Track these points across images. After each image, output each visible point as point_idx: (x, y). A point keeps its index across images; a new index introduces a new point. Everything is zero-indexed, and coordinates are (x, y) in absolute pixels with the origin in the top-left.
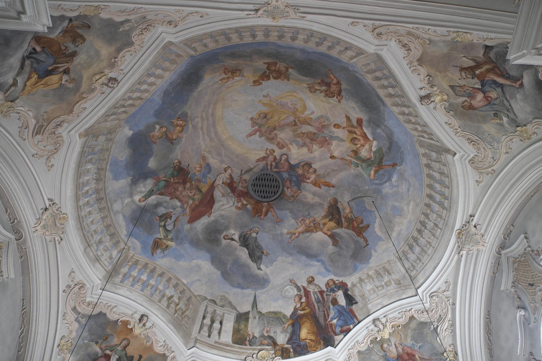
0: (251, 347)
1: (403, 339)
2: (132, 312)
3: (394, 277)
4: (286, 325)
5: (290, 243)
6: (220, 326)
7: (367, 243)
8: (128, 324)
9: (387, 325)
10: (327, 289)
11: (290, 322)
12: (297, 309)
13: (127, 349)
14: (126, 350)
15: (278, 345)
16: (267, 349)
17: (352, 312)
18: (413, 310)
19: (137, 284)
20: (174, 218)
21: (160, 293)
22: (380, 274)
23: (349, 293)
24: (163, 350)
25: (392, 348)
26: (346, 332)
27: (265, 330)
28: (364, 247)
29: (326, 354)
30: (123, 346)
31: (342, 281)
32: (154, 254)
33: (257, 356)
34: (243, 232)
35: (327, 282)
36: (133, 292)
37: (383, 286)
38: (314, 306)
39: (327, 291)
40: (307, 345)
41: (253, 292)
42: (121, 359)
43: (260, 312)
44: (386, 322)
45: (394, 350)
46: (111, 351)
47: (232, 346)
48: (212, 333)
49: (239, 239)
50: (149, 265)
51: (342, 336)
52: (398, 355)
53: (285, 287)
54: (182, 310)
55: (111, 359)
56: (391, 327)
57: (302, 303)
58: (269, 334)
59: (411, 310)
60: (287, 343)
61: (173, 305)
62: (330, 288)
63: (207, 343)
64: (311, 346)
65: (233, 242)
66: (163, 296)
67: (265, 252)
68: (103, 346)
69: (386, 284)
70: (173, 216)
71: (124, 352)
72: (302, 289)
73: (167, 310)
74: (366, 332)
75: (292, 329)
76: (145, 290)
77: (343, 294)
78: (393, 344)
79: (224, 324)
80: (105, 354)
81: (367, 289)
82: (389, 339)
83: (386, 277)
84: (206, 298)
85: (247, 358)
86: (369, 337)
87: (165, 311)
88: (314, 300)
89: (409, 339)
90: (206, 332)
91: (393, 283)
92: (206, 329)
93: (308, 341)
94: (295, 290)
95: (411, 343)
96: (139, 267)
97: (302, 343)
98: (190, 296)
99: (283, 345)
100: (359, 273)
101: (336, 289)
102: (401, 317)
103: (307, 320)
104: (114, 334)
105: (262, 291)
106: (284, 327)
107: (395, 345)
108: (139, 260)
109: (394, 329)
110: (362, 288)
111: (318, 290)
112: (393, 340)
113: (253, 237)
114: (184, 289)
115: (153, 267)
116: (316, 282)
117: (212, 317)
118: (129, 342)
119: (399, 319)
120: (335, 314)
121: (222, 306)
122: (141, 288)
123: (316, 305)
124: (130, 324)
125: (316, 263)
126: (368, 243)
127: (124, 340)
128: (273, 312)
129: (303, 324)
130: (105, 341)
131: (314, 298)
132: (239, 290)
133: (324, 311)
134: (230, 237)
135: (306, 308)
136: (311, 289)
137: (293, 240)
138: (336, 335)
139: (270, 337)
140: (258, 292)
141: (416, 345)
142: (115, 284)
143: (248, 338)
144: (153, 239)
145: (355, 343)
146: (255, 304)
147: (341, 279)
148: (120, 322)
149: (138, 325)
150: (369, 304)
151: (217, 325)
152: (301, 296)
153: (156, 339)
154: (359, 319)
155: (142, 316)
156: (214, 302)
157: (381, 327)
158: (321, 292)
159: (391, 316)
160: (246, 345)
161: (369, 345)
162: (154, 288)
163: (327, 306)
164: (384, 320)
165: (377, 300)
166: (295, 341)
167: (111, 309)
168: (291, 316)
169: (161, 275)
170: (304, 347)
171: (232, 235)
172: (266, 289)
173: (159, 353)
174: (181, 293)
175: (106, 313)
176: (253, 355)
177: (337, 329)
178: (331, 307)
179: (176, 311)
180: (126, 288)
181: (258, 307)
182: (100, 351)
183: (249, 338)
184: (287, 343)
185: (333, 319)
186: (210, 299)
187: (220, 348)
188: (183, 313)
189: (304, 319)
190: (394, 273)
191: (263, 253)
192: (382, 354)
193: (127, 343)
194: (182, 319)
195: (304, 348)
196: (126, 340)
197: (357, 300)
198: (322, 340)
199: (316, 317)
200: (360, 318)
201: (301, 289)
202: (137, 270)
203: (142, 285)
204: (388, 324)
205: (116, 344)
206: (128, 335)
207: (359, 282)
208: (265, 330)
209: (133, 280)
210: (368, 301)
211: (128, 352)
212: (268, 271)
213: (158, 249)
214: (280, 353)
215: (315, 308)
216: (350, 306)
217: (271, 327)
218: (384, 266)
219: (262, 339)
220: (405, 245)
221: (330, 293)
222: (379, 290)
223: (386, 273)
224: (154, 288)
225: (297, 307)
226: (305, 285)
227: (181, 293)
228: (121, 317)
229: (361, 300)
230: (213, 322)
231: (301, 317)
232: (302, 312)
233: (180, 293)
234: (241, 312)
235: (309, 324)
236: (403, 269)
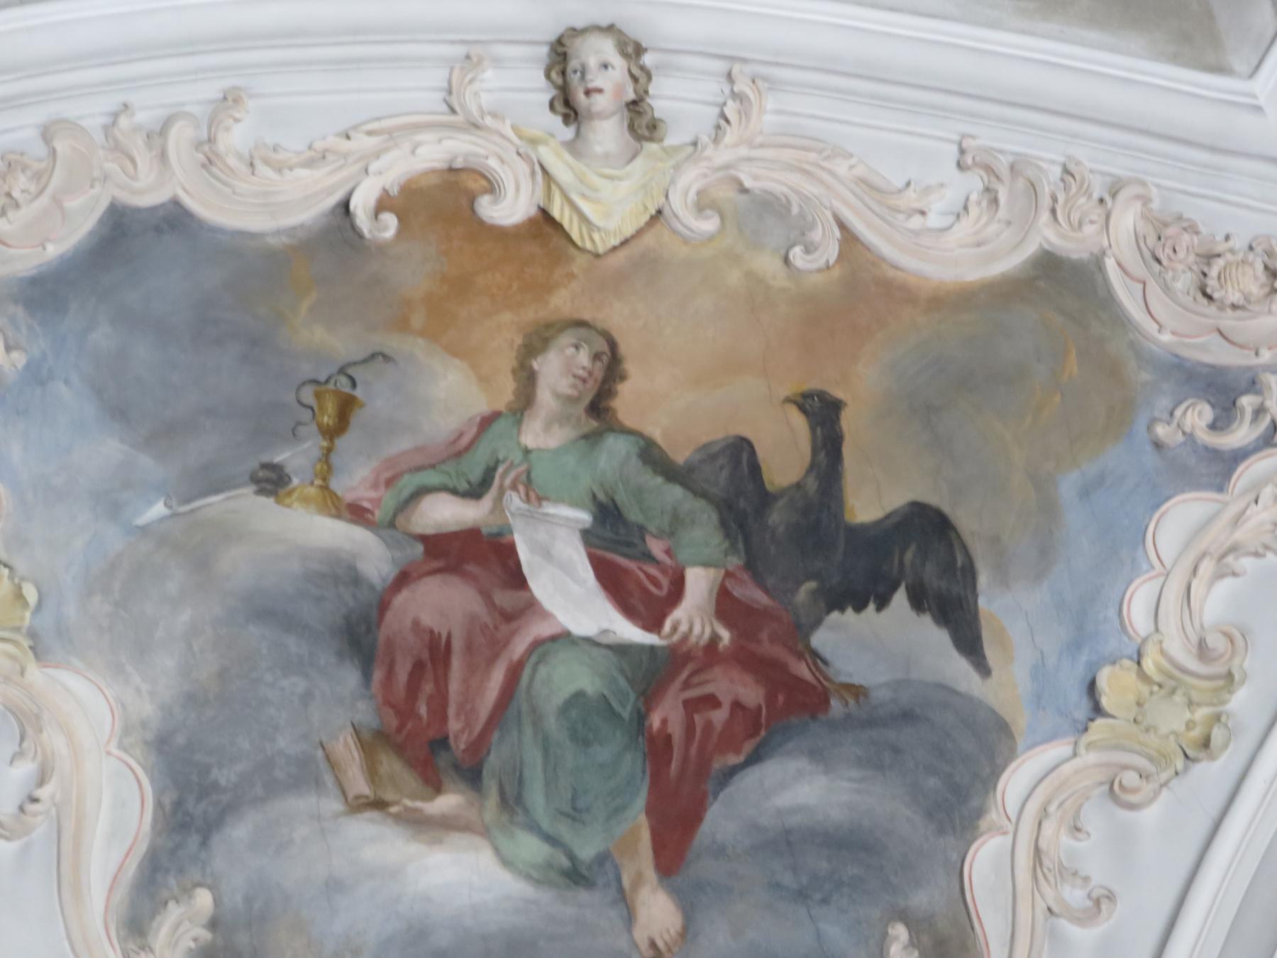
2: (438, 77)
13: (625, 403)
30: (571, 400)
42: (634, 515)
46: (475, 492)
71: (617, 448)
80: (424, 539)
104: (392, 343)
118: (602, 346)
124: (492, 187)
130: (342, 442)
149: (573, 146)
153: (867, 185)
167: (198, 146)
175: (176, 202)
193: (584, 358)
196: (566, 339)
205: (480, 405)
206: (547, 288)
211: (656, 433)
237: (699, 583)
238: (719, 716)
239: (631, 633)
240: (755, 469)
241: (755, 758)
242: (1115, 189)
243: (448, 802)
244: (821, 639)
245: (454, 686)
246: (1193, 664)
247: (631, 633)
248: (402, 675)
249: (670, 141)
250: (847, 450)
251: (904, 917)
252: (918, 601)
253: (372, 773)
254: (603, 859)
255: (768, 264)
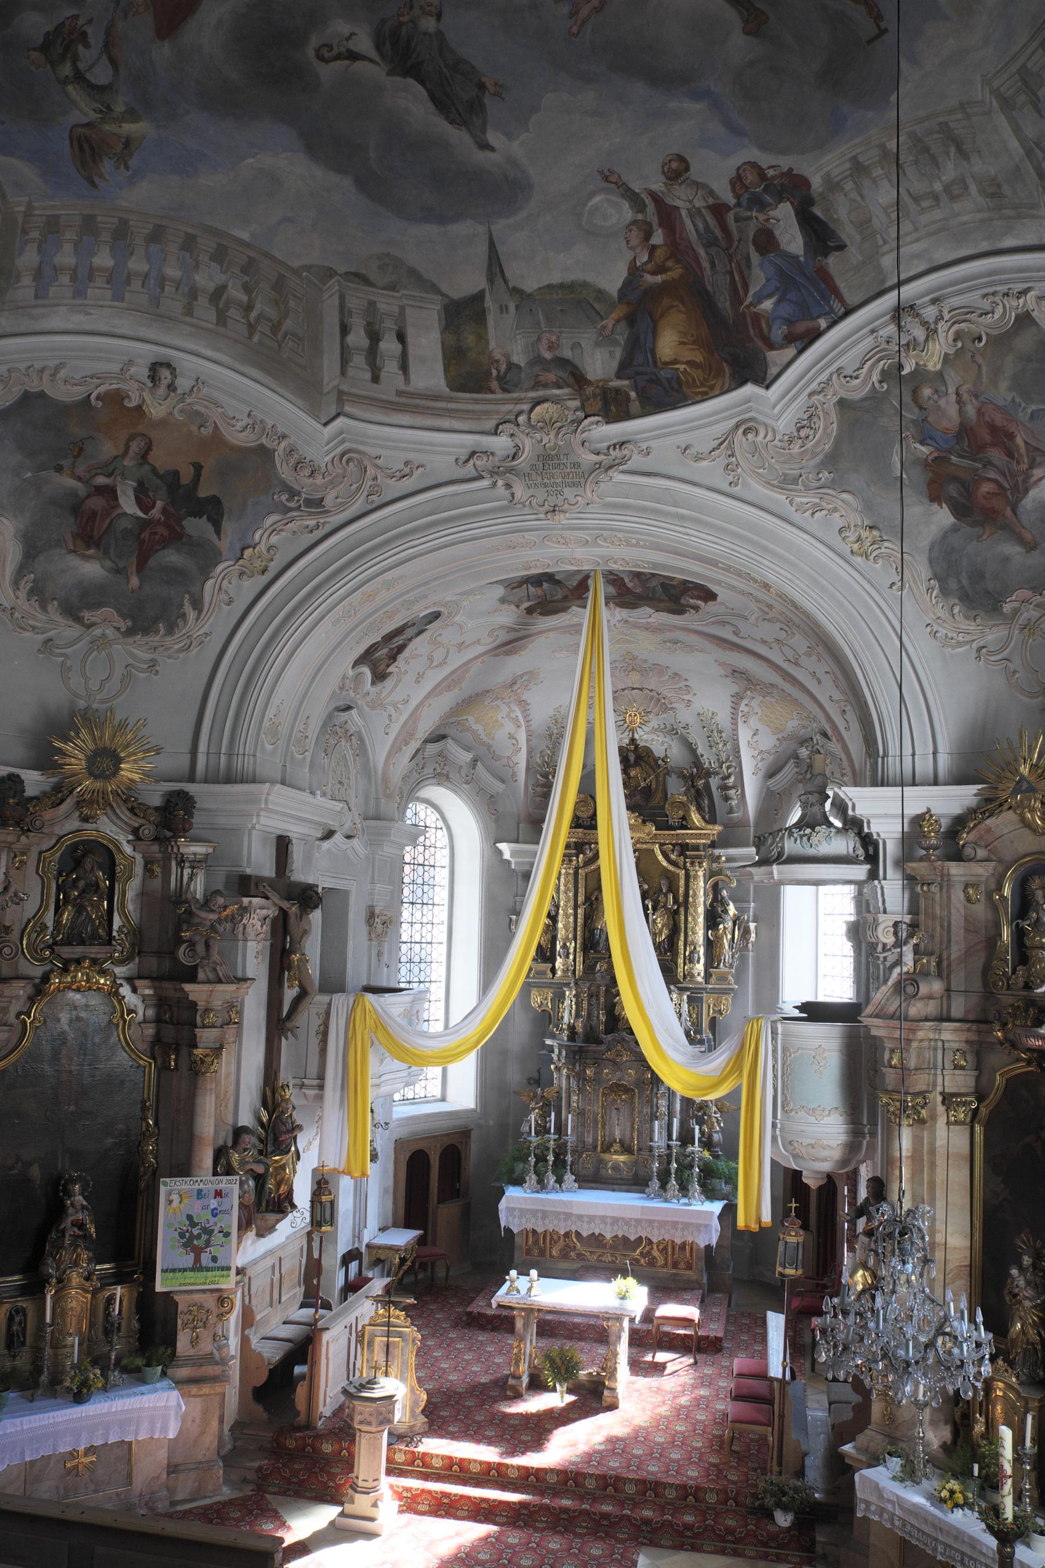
0: (507, 396)
1: (984, 380)
3: (978, 166)
4: (609, 322)
5: (576, 35)
6: (400, 346)
7: (878, 26)
8: (123, 399)
9: (940, 331)
10: (738, 197)
11: (620, 311)
12: (638, 269)
13: (152, 457)
14: (150, 461)
15: (589, 383)
16: (558, 396)
17: (825, 277)
18: (1032, 293)
19: (91, 284)
20: (96, 36)
21: (177, 289)
22: (927, 150)
23: (817, 211)
24: (253, 437)
25: (947, 402)
26: (806, 340)
27: (544, 342)
28: (870, 41)
29: (740, 406)
31: (791, 170)
32: (96, 179)
33: (529, 418)
34: (383, 21)
35: (733, 174)
36: (91, 311)
37: (936, 198)
38: (697, 257)
39: (738, 205)
40: (678, 378)
41: (481, 229)
43: (516, 291)
44: (936, 322)
45: (952, 410)
46: (109, 476)
47: (450, 399)
48: (380, 370)
49: (378, 48)
50: (99, 219)
51: (791, 352)
52: (961, 424)
53: (589, 198)
54: (270, 320)
55: (119, 492)
56: (951, 336)
57: (654, 248)
58: (558, 353)
59: (1024, 292)
60: (619, 375)
61: (233, 313)
62: (746, 196)
63: (376, 400)
64: (694, 380)
65: (359, 66)
66: (193, 294)
67: (488, 82)
68: (80, 470)
69: (947, 188)
70: (89, 30)
71: (147, 467)
72: (648, 201)
73: (222, 330)
74: (869, 342)
75: (627, 332)
76: (127, 295)
77: (797, 214)
78: (951, 390)
79: (410, 339)
81: (880, 201)
82: (940, 375)
83: (950, 165)
84: (330, 273)
85: (501, 427)
86: (880, 360)
87: (216, 333)
88: (693, 236)
89: (1004, 385)
90: (362, 369)
91: (973, 188)
92: (359, 360)
93: (682, 367)
94: (626, 205)
95: (1009, 399)
96: (70, 235)
97: (663, 374)
98: (280, 274)
99: (606, 381)
100: (853, 143)
101: (768, 198)
102: (988, 308)
103: (676, 303)
105: (512, 220)
106: (604, 328)
107: (957, 394)
108: (57, 217)
109: (959, 345)
110: (862, 197)
111: (705, 204)
112: (953, 380)
113: (430, 35)
114: (249, 257)
115: (116, 220)
116: (694, 173)
117: (369, 324)
118: (148, 441)
119: (981, 315)
120: (768, 280)
121: (392, 287)
122: (110, 292)
123: (702, 252)
124: (128, 396)
125: (689, 105)
126: (883, 25)
127: (132, 438)
128: (562, 286)
129: (662, 316)
131: (694, 232)
132: (432, 230)
133: (731, 273)
134: (343, 50)
135: (670, 264)
136: (681, 198)
137: (584, 22)
138: (772, 347)
139: (562, 363)
140: (499, 227)
141: (1023, 405)
142: (21, 308)
143: (494, 372)
144: (67, 134)
145: (831, 375)
146: (495, 266)
147: (785, 162)
148: (98, 398)
149: (152, 394)
150: (883, 255)
151: (389, 345)
152: (650, 225)
153: (224, 415)
154: (848, 302)
155: (155, 368)
156: (365, 280)
157: (919, 333)
158: (719, 210)
159: (956, 301)
160: (492, 392)
161: (877, 385)
162: (152, 282)
163: (739, 257)
164: (930, 313)
165: (912, 243)
166: (640, 369)
168: (622, 292)
169: (156, 235)
170: (669, 383)
171: (348, 39)
172: (522, 214)
173: (247, 448)
174: (245, 270)
176: (517, 416)
177: (774, 328)
178: (755, 257)
179: (252, 328)
180: (63, 309)
181: (508, 274)
182: (79, 484)
183: (499, 371)
184: (619, 375)
185: (760, 298)
186: (346, 273)
187: (417, 406)
188: (275, 328)
189: (666, 302)
190: (979, 152)
191: (482, 87)
192: (911, 414)
193: (143, 444)
194: (280, 346)
195: (672, 388)
196: (139, 438)
197: (844, 236)
198: (726, 361)
199: (706, 291)
200: (852, 299)
201: (647, 201)
202: (68, 247)
203: (108, 282)
204: (942, 327)
205: (115, 453)
207: (851, 175)
208: (544, 342)
209: (74, 278)
210: (881, 242)
212: (516, 148)
213: (102, 161)
214: (598, 404)
215: (699, 264)
216: (820, 258)
217: (561, 332)
218: (947, 123)
219: (537, 369)
220: (1035, 45)
221: (749, 214)
222: (923, 211)
223: (953, 149)
224: (152, 282)
225: (638, 264)
226: (658, 185)
227: (245, 270)
228: (93, 386)
229: (858, 238)
230: (374, 337)
231: (654, 294)
232: (659, 279)
233: (242, 272)
234: (456, 295)
235: (682, 316)
236: (1014, 144)
237: (159, 504)
238: (157, 537)
239: (141, 514)
240: (179, 479)
241: (163, 548)
242: (284, 437)
243: (91, 552)
244: (184, 523)
245: (97, 524)
246: (265, 552)
247: (141, 514)
248: (85, 520)
249: (179, 392)
250: (202, 479)
251: (188, 592)
252: (209, 519)
253: (74, 545)
254: (125, 567)
255: (194, 428)
